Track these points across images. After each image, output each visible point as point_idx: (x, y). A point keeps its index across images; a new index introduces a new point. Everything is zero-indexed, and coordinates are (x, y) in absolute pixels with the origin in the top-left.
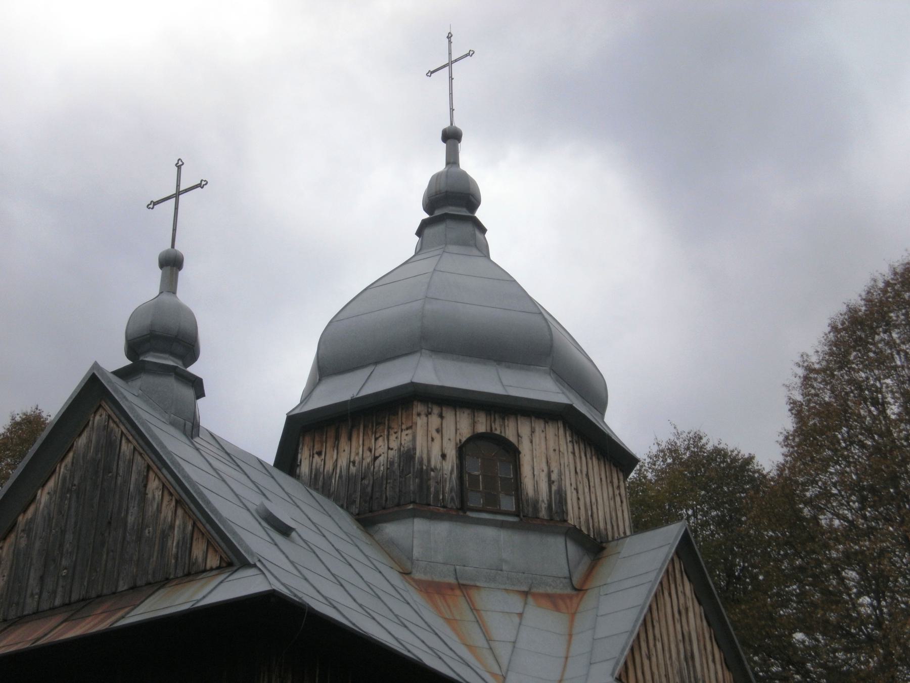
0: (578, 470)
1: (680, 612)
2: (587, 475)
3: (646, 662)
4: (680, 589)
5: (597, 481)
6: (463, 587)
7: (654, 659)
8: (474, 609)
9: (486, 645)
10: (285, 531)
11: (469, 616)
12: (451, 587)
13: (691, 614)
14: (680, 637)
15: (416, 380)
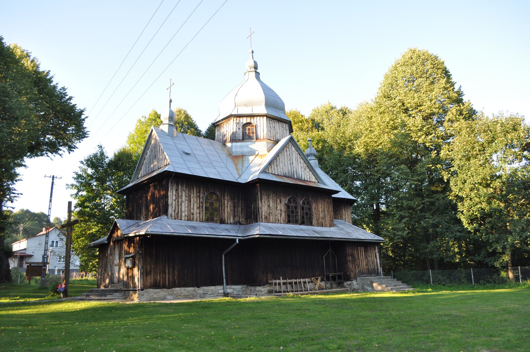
0: (271, 127)
1: (289, 155)
2: (274, 127)
3: (276, 168)
4: (290, 150)
5: (278, 128)
6: (243, 156)
7: (279, 167)
8: (243, 161)
9: (241, 168)
10: (188, 154)
11: (241, 162)
12: (240, 156)
13: (294, 154)
14: (289, 160)
15: (232, 113)
